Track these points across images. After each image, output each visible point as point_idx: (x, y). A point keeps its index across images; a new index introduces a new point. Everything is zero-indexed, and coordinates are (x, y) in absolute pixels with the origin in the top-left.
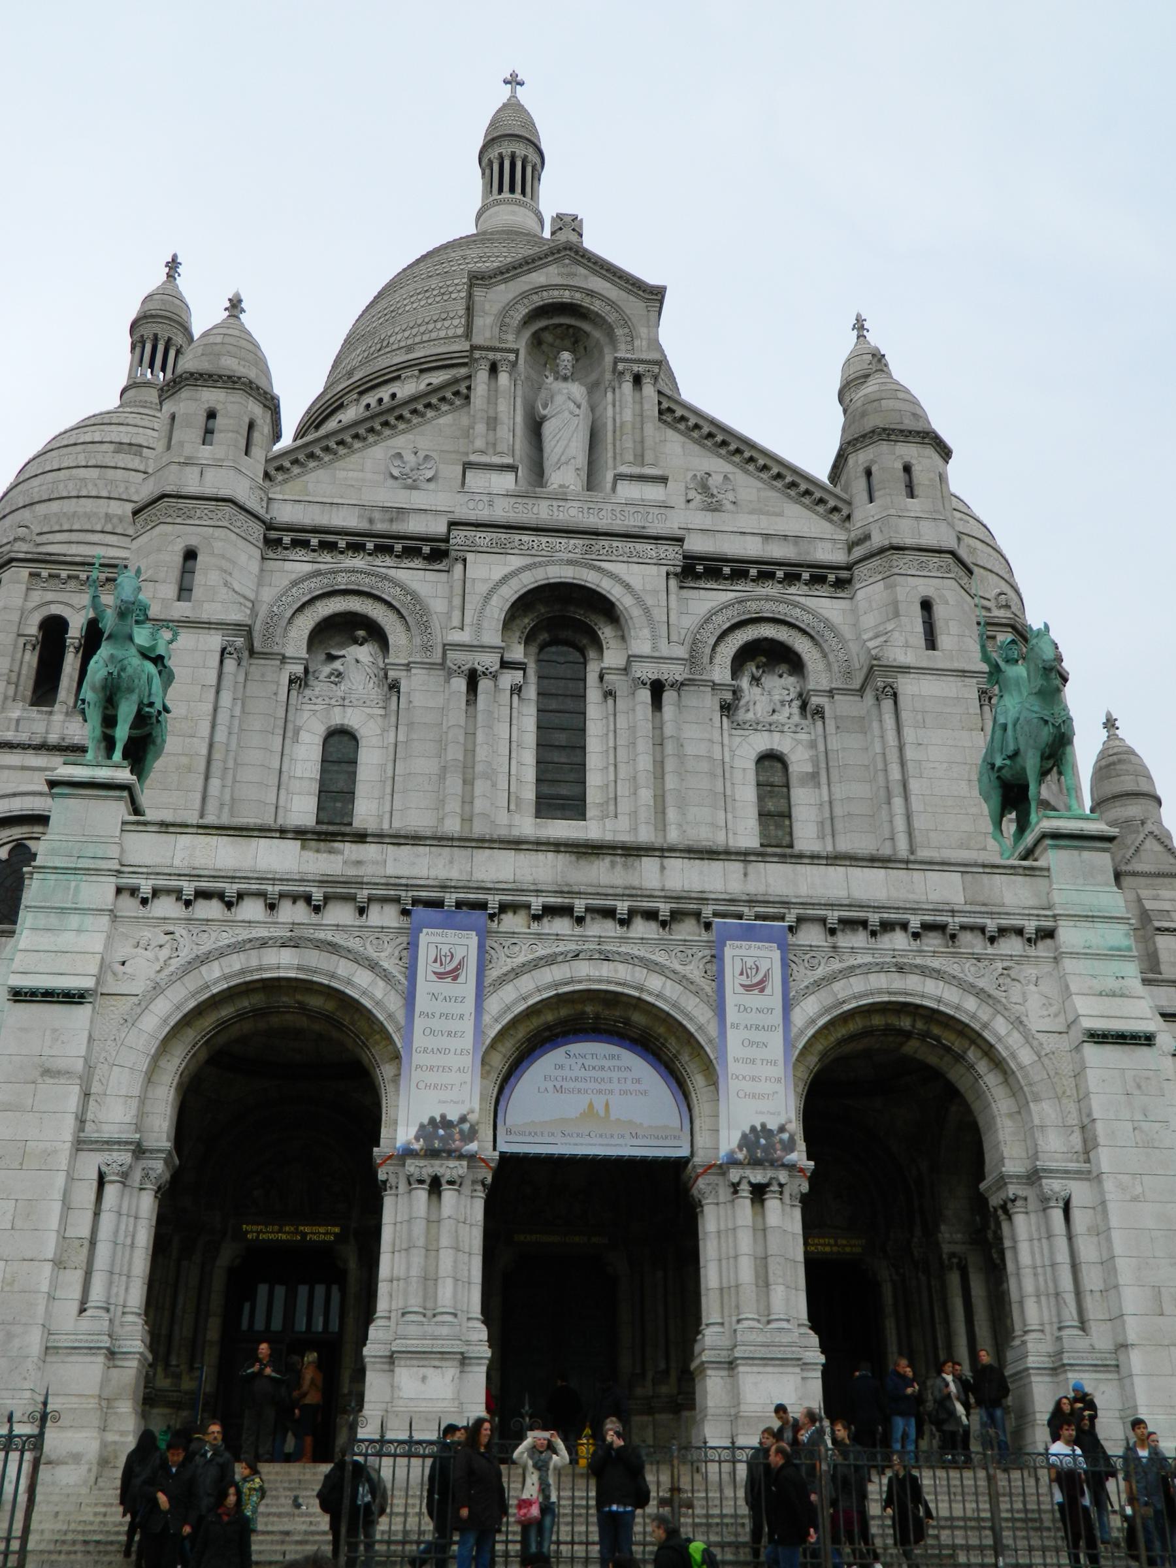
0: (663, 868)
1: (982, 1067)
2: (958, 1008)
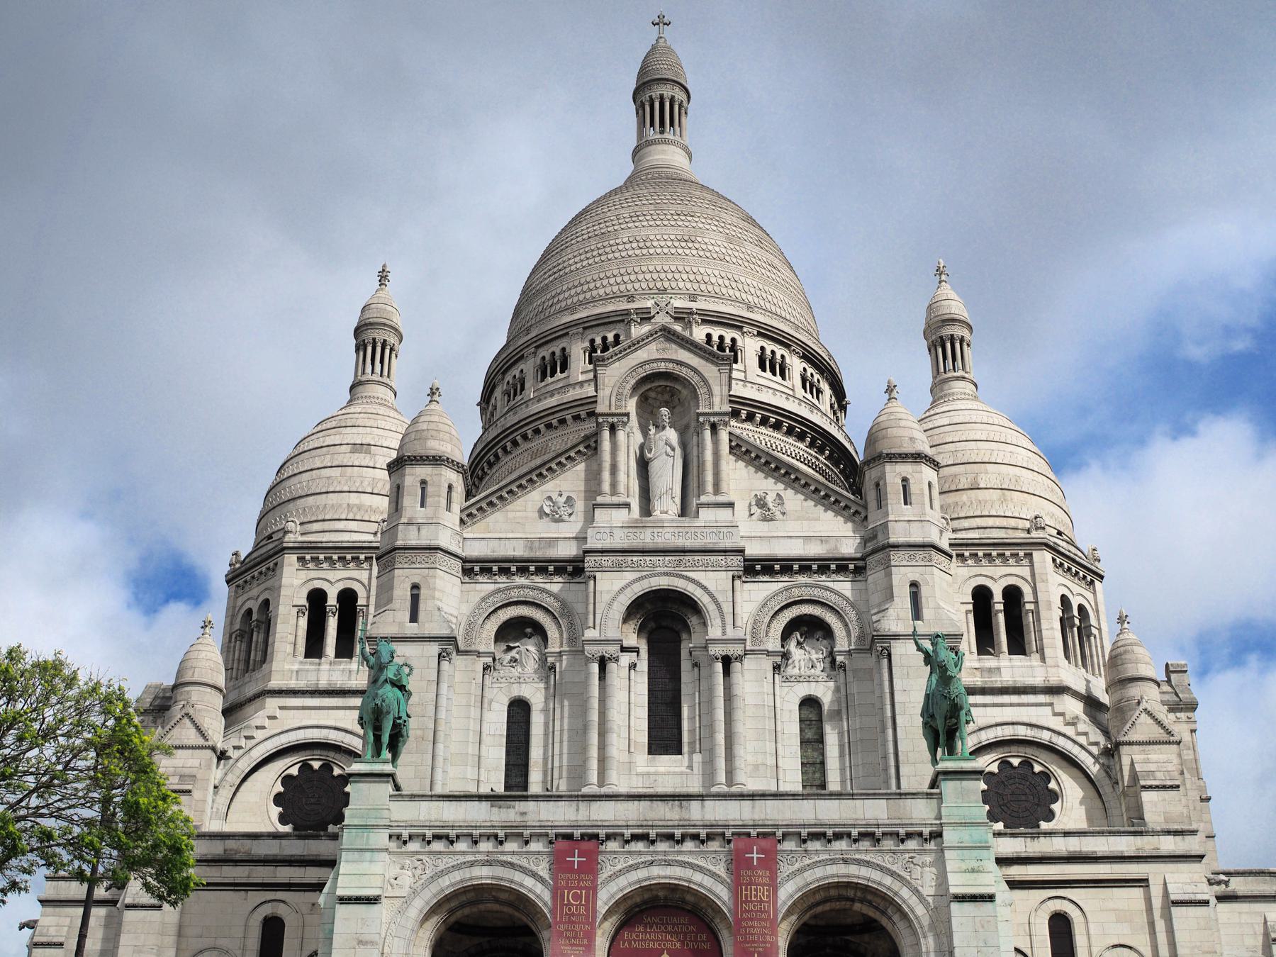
0: (703, 806)
1: (896, 918)
2: (880, 884)
